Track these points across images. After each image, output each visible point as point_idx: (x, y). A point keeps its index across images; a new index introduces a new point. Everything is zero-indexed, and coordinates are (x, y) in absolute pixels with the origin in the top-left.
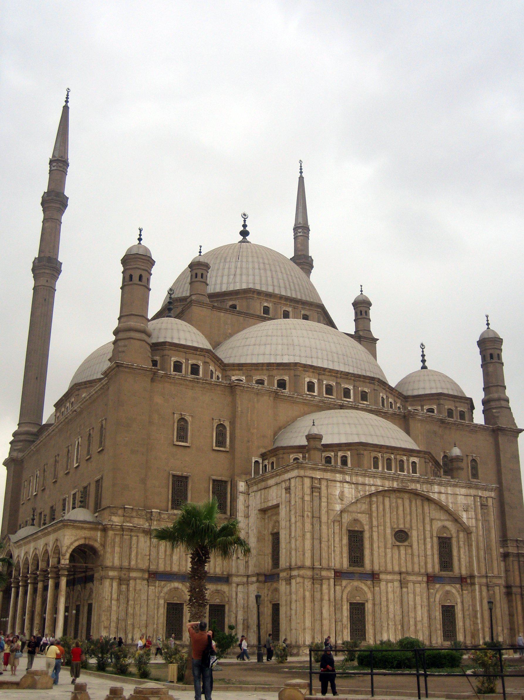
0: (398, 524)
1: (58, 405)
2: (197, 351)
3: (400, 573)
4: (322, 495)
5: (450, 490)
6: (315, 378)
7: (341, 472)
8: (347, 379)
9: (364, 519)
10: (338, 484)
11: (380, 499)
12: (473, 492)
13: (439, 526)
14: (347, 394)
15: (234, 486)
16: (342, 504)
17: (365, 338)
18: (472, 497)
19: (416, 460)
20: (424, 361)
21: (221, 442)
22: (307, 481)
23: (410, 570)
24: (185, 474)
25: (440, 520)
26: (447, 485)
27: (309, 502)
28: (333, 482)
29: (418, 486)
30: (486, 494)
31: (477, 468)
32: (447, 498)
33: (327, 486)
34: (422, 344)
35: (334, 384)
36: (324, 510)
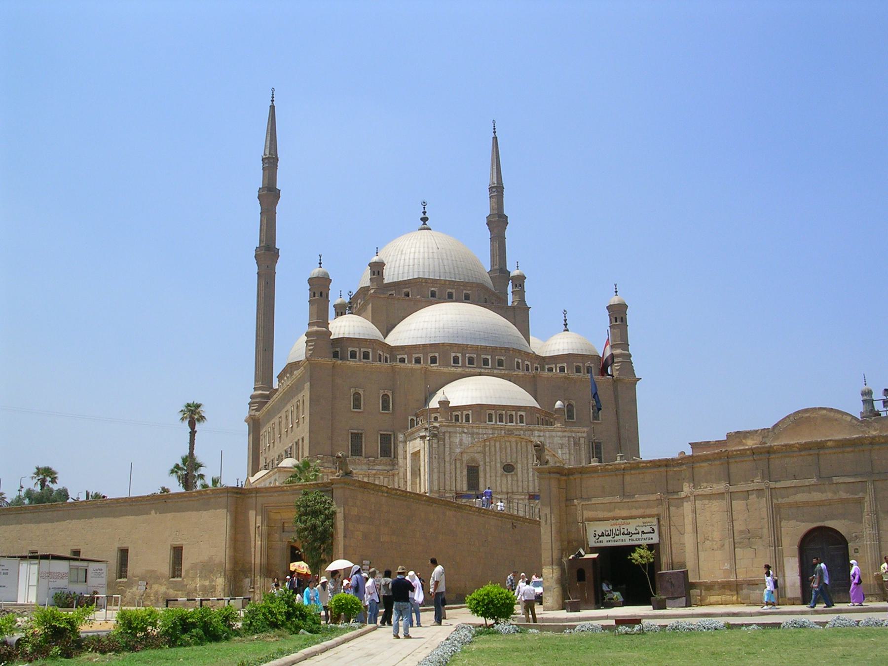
1: (280, 377)
3: (508, 493)
7: (459, 427)
9: (479, 457)
11: (492, 443)
12: (566, 434)
14: (486, 362)
15: (396, 438)
19: (523, 413)
20: (566, 325)
21: (385, 407)
23: (515, 490)
26: (544, 431)
30: (580, 435)
33: (450, 437)
36: (447, 453)
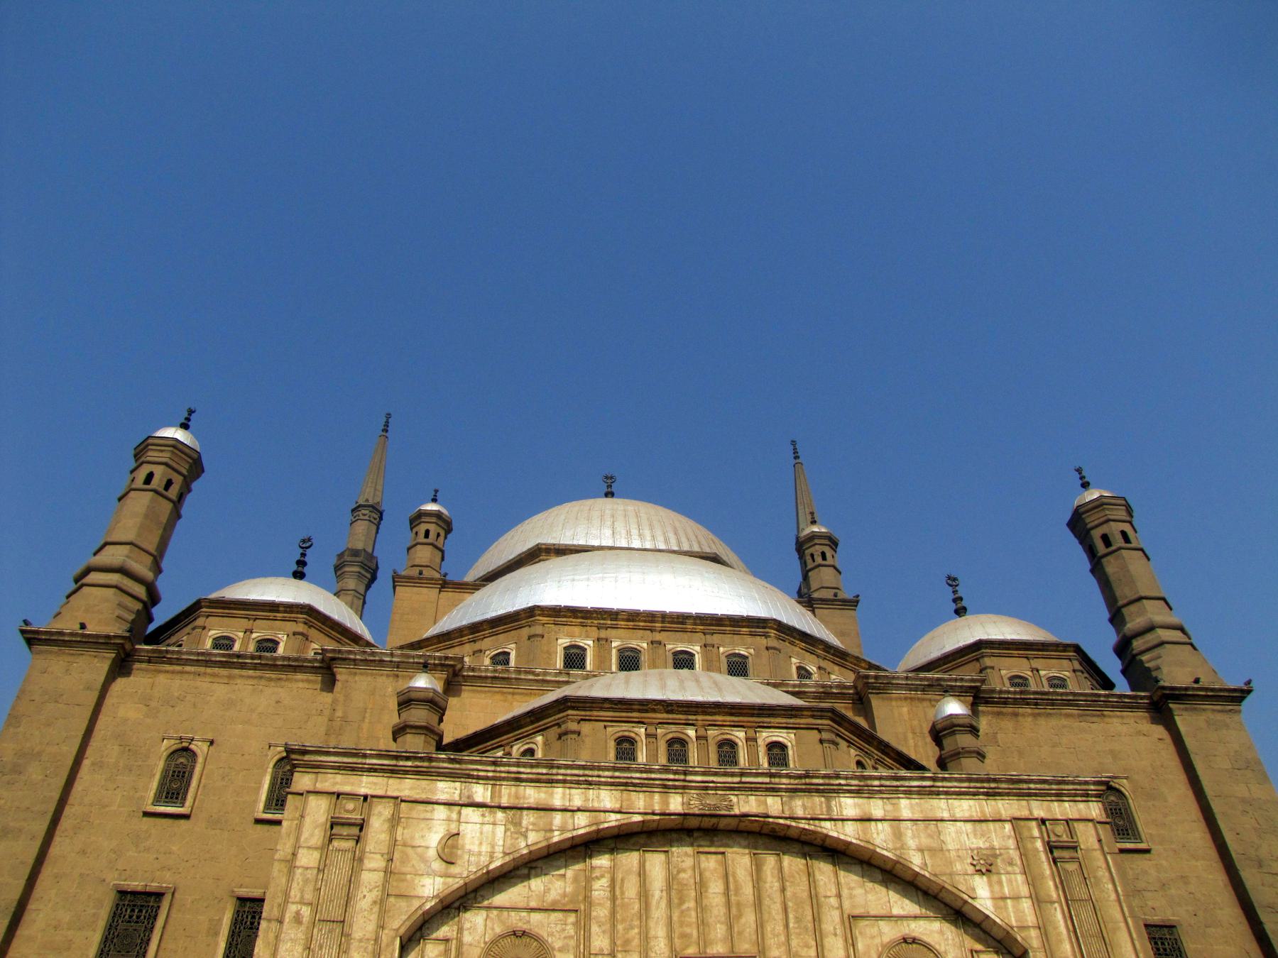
0: (704, 939)
2: (278, 611)
4: (370, 847)
5: (906, 807)
6: (587, 637)
8: (684, 631)
10: (441, 812)
13: (886, 939)
16: (447, 876)
17: (824, 601)
18: (1008, 826)
22: (318, 810)
24: (154, 886)
25: (889, 917)
27: (311, 874)
28: (421, 807)
29: (773, 805)
30: (1067, 809)
31: (1127, 808)
32: (898, 835)
33: (395, 821)
34: (949, 578)
35: (645, 645)
36: (366, 898)
